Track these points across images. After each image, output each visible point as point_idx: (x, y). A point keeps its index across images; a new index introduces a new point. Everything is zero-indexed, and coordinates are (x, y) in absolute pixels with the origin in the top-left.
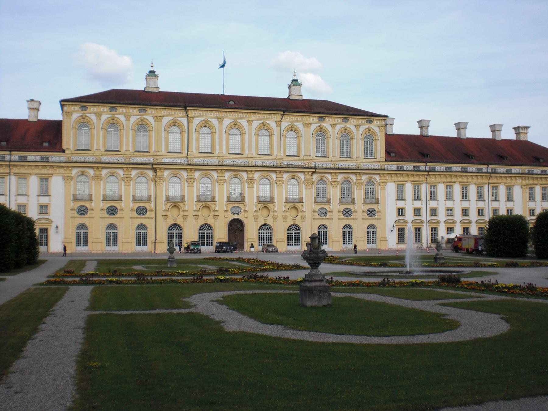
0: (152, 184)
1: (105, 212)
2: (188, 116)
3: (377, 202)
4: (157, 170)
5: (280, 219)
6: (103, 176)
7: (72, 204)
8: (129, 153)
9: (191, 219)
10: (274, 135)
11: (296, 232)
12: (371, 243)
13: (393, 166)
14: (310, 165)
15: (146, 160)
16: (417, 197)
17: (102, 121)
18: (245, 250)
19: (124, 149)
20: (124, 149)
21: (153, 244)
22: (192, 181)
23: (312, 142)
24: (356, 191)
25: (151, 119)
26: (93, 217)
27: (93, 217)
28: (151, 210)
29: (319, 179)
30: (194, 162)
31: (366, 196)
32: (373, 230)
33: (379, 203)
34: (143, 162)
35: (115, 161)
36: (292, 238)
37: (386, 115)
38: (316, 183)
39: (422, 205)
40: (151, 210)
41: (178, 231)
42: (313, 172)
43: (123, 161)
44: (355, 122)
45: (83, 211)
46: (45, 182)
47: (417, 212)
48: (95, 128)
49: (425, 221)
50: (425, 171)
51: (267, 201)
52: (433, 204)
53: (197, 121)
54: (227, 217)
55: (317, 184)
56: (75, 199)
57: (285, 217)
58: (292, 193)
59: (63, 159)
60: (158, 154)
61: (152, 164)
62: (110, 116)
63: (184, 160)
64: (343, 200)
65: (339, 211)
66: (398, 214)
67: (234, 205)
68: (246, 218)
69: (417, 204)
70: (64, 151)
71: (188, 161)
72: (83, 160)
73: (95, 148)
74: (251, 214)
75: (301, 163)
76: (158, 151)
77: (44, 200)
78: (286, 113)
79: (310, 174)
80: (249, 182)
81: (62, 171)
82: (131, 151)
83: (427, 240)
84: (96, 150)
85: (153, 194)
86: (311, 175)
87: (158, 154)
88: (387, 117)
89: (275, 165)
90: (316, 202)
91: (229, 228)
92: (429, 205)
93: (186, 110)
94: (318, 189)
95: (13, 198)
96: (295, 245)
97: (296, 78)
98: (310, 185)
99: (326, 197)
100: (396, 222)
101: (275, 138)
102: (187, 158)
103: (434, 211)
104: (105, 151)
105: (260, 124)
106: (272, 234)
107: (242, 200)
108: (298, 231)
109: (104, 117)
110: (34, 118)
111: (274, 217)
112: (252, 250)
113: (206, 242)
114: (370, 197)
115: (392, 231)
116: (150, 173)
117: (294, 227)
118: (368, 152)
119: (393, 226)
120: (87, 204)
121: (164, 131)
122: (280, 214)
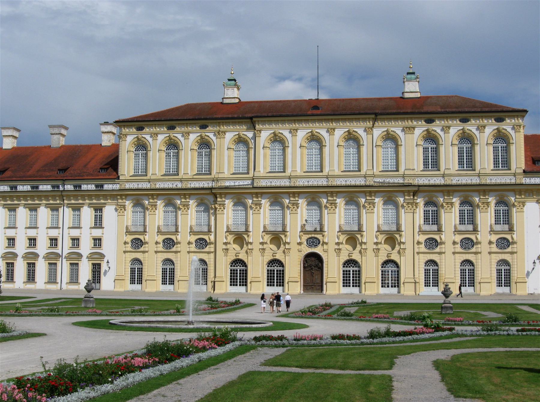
1: (161, 245)
3: (511, 230)
9: (256, 253)
12: (503, 286)
15: (205, 183)
28: (211, 243)
36: (469, 278)
37: (525, 109)
41: (355, 268)
45: (138, 243)
46: (99, 212)
54: (301, 251)
56: (128, 232)
57: (377, 251)
59: (117, 187)
60: (221, 176)
67: (310, 236)
68: (325, 251)
74: (332, 247)
77: (97, 233)
78: (379, 117)
79: (412, 194)
91: (304, 264)
95: (66, 231)
109: (161, 137)
110: (108, 142)
113: (275, 281)
119: (534, 263)
120: (173, 237)
122: (370, 246)
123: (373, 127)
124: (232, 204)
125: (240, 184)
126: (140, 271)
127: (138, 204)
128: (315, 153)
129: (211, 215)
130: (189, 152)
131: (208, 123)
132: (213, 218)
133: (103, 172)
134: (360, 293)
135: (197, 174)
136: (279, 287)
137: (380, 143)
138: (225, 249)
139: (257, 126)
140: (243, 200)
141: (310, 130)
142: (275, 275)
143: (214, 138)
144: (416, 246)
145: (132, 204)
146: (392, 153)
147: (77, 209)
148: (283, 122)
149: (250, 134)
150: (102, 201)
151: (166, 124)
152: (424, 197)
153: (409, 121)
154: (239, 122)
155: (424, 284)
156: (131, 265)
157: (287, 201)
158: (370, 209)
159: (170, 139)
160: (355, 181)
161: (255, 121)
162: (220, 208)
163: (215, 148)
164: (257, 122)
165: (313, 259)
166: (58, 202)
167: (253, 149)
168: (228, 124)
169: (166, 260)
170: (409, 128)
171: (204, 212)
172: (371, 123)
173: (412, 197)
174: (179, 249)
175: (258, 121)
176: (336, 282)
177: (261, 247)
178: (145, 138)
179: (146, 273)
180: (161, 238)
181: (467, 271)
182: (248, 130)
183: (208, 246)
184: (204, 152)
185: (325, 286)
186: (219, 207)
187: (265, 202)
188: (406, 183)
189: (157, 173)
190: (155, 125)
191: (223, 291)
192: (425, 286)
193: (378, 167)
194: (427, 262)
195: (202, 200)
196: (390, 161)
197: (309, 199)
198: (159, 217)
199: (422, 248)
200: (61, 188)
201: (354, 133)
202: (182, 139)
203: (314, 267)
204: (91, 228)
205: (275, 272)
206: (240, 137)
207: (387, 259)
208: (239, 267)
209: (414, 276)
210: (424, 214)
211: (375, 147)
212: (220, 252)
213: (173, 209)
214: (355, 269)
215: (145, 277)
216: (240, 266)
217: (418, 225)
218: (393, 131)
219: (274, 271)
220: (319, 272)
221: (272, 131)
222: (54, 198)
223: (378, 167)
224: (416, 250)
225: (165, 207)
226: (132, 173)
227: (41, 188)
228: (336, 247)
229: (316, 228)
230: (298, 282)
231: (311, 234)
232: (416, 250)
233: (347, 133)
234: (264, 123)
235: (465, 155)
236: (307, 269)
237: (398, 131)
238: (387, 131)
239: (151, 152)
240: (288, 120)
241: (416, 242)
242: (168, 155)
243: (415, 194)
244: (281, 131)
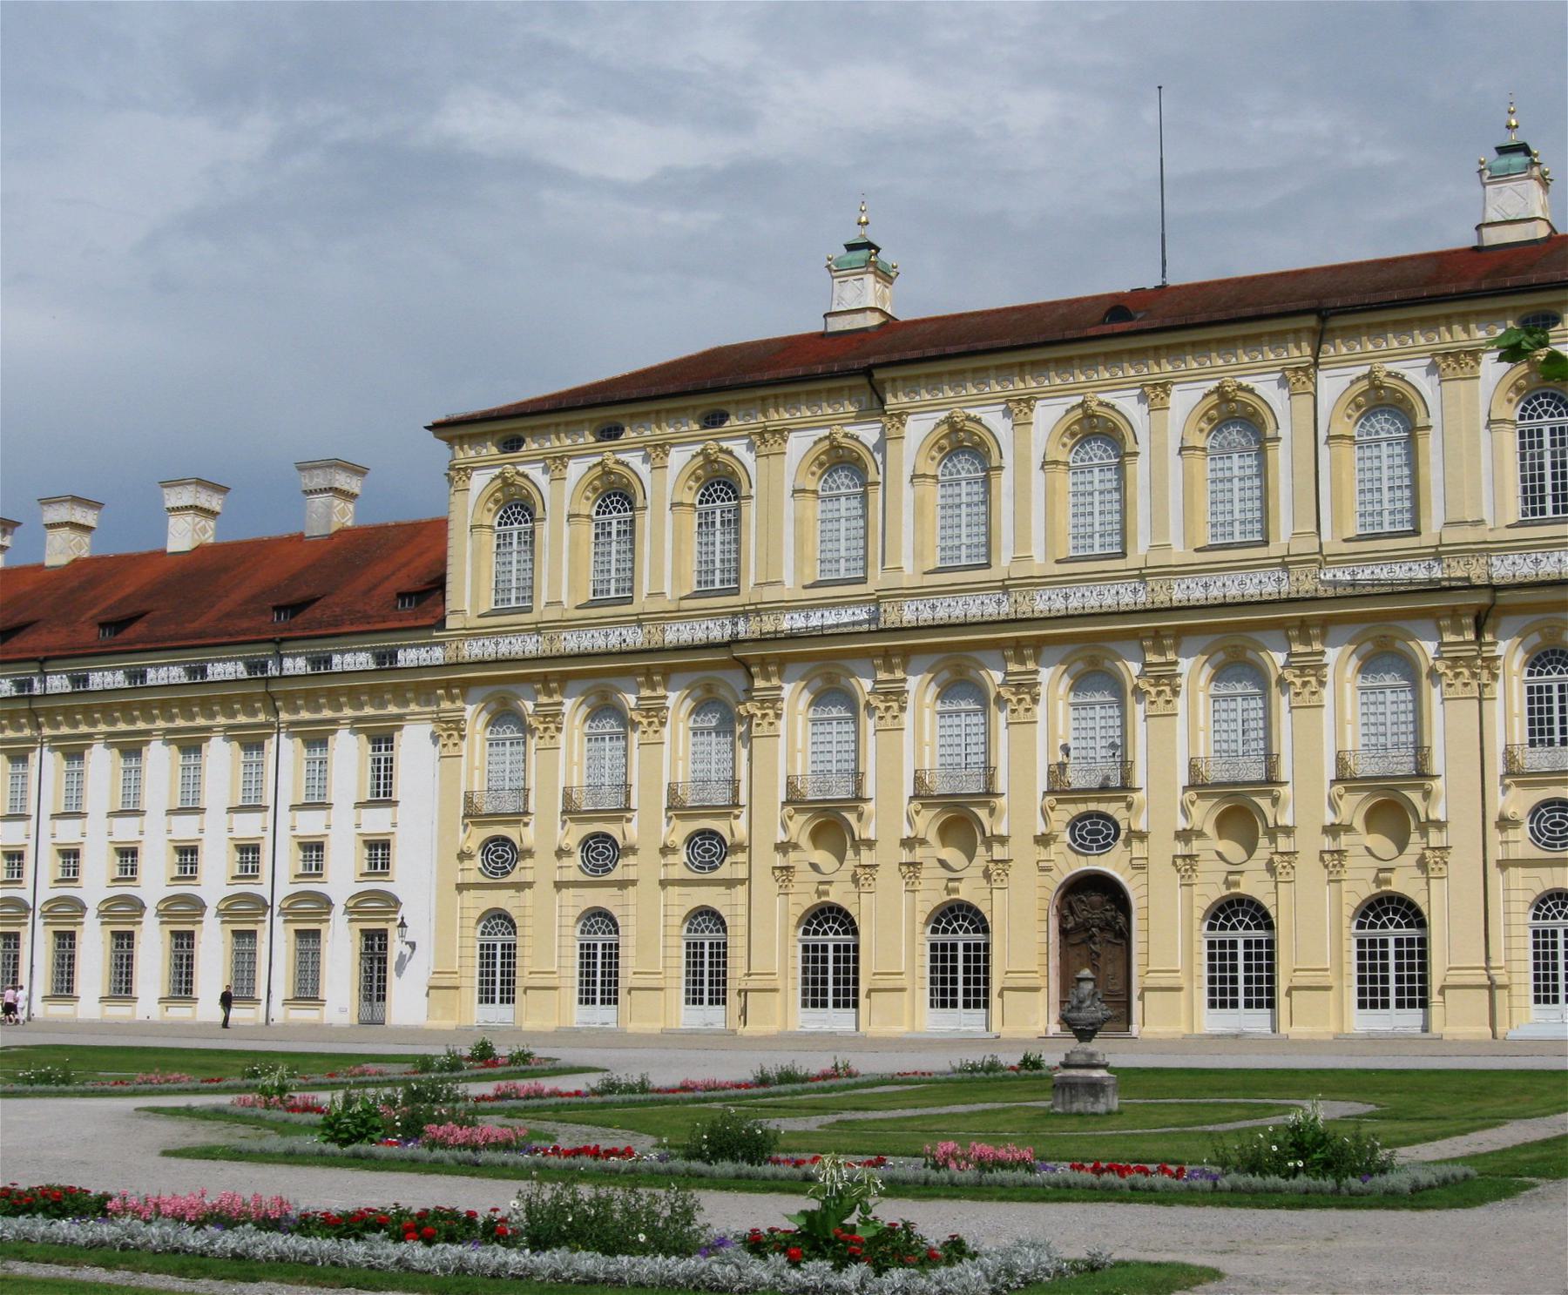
1: (577, 859)
5: (1308, 868)
9: (889, 878)
19: (646, 590)
20: (646, 590)
28: (739, 848)
56: (473, 815)
60: (769, 594)
67: (1082, 808)
68: (1139, 867)
74: (1162, 849)
77: (377, 822)
78: (1335, 322)
79: (1468, 621)
91: (1062, 919)
96: (1400, 1004)
122: (1310, 843)
123: (1316, 364)
124: (806, 697)
125: (856, 618)
126: (720, 952)
127: (504, 715)
128: (1242, 473)
129: (739, 744)
130: (668, 513)
131: (728, 403)
132: (743, 754)
133: (408, 608)
134: (1274, 1031)
135: (696, 595)
136: (972, 1010)
137: (1345, 427)
138: (781, 868)
139: (890, 399)
140: (972, 673)
141: (1079, 399)
142: (960, 964)
143: (748, 458)
144: (1494, 835)
145: (485, 717)
146: (1398, 461)
147: (316, 739)
148: (980, 376)
149: (869, 434)
150: (392, 709)
152: (1523, 634)
153: (1457, 328)
154: (830, 391)
155: (1532, 993)
156: (483, 933)
157: (998, 676)
158: (1306, 691)
159: (607, 473)
160: (1242, 583)
161: (883, 382)
162: (764, 716)
163: (753, 492)
164: (888, 386)
165: (1096, 898)
166: (261, 718)
167: (880, 487)
168: (791, 401)
169: (594, 916)
170: (1456, 355)
171: (718, 734)
172: (1307, 350)
173: (1470, 636)
174: (631, 874)
175: (894, 380)
176: (1179, 989)
177: (905, 856)
178: (526, 477)
179: (527, 961)
180: (573, 835)
182: (861, 417)
183: (728, 860)
184: (718, 512)
185: (1136, 1005)
186: (759, 713)
187: (919, 687)
189: (564, 598)
190: (557, 425)
191: (773, 1028)
192: (1537, 1000)
193: (1337, 522)
194: (1544, 902)
195: (709, 688)
196: (1386, 495)
197: (1079, 666)
198: (674, 750)
199: (1521, 842)
200: (273, 671)
201: (1241, 396)
202: (643, 469)
203: (1102, 930)
204: (360, 805)
205: (961, 953)
206: (835, 447)
207: (1375, 890)
208: (831, 936)
209: (1487, 958)
211: (1326, 443)
212: (764, 882)
213: (618, 726)
214: (1406, 932)
216: (837, 933)
217: (1500, 749)
218: (1396, 376)
219: (954, 947)
220: (1118, 949)
221: (943, 415)
222: (248, 704)
223: (1337, 522)
224: (1496, 853)
225: (593, 721)
226: (488, 604)
227: (153, 677)
228: (1180, 848)
229: (1107, 778)
230: (1036, 989)
231: (1085, 801)
232: (1496, 853)
233: (1214, 399)
234: (911, 384)
236: (1075, 939)
237: (1416, 373)
238: (1370, 376)
239: (546, 524)
240: (998, 368)
241: (1492, 818)
243: (1481, 622)
244: (973, 412)
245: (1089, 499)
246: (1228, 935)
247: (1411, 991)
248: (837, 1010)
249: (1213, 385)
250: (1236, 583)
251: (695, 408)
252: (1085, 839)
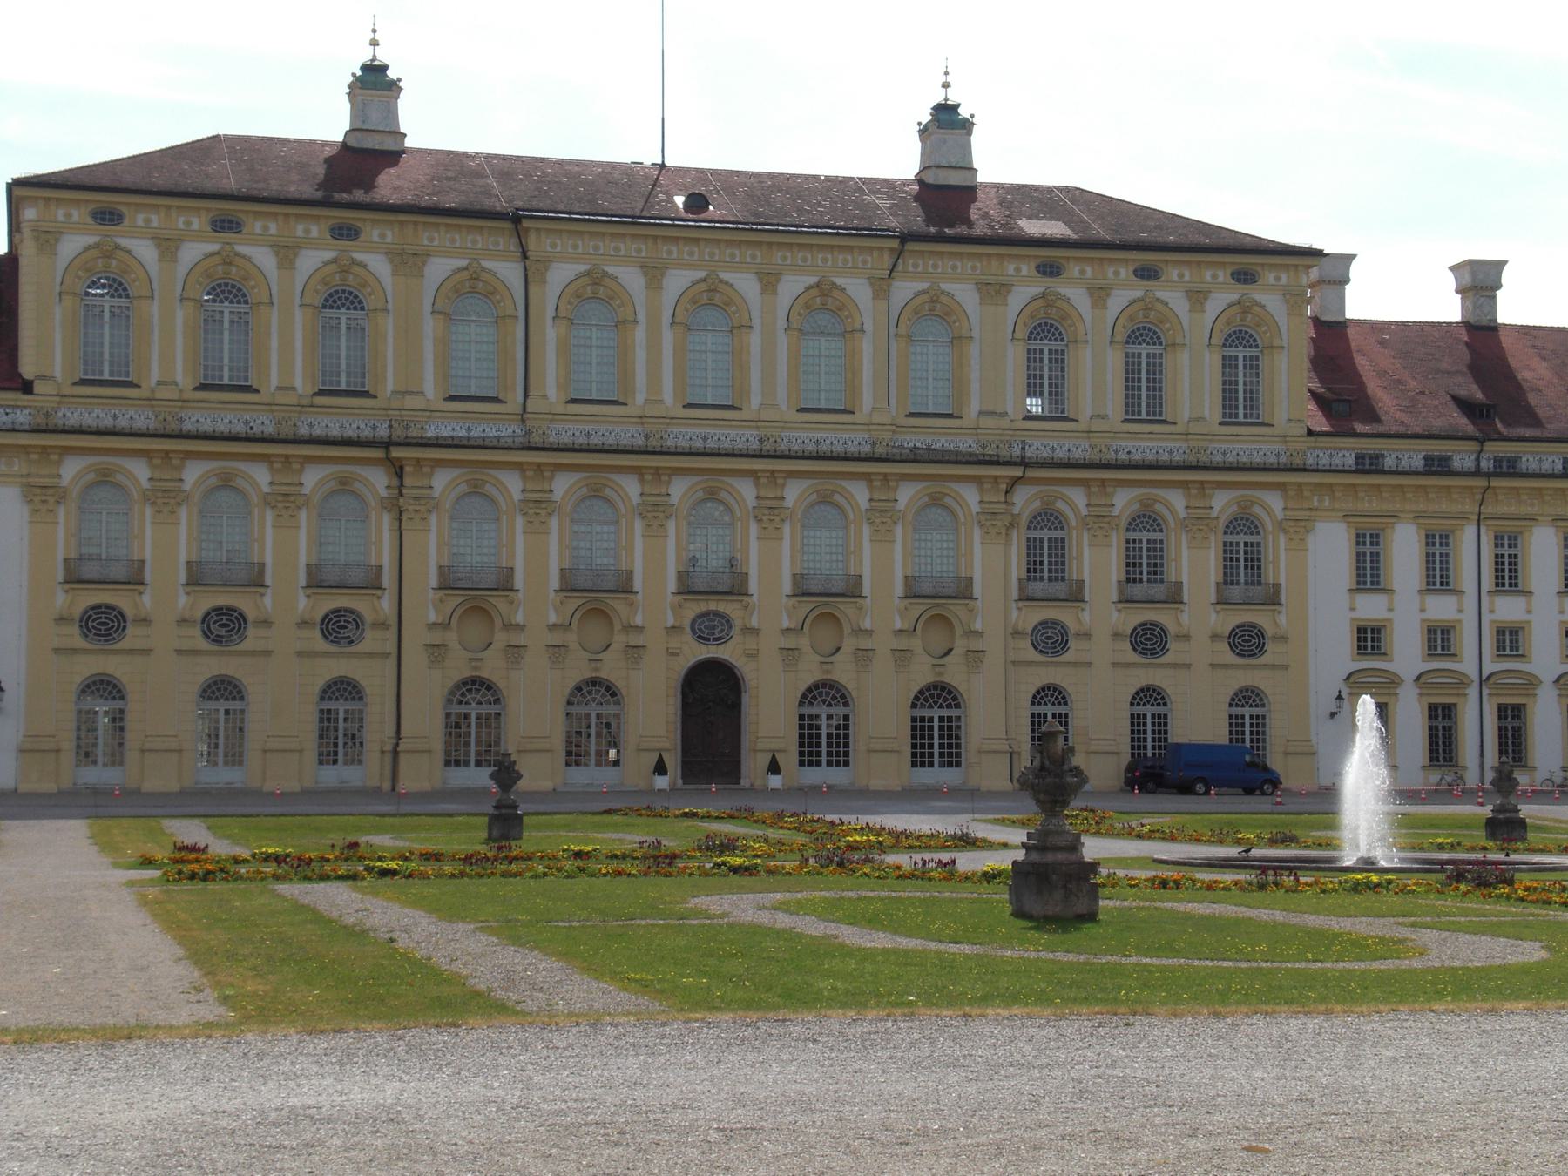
0: (387, 520)
2: (525, 255)
3: (1273, 599)
4: (408, 469)
6: (187, 486)
7: (61, 599)
8: (291, 399)
10: (862, 330)
11: (946, 713)
13: (1344, 453)
14: (1004, 453)
15: (362, 426)
16: (1438, 577)
17: (182, 271)
18: (744, 782)
19: (274, 382)
20: (274, 382)
21: (388, 758)
22: (543, 512)
23: (1014, 359)
24: (1185, 553)
25: (379, 266)
26: (146, 652)
27: (146, 652)
28: (381, 625)
29: (1037, 504)
30: (552, 439)
31: (1225, 574)
32: (1256, 711)
33: (1280, 604)
34: (350, 433)
35: (239, 428)
38: (1024, 521)
39: (1460, 611)
40: (381, 625)
42: (1015, 481)
43: (270, 430)
44: (1187, 278)
47: (1439, 639)
48: (156, 294)
49: (1474, 676)
50: (1477, 473)
51: (834, 590)
52: (1508, 609)
53: (561, 274)
54: (677, 655)
55: (1029, 528)
57: (902, 657)
58: (929, 560)
59: (22, 417)
60: (410, 402)
61: (387, 444)
62: (215, 247)
63: (510, 430)
64: (1137, 590)
65: (1116, 635)
66: (1359, 648)
67: (703, 607)
69: (1441, 608)
70: (27, 387)
71: (528, 433)
72: (107, 422)
73: (155, 375)
75: (966, 444)
76: (411, 393)
78: (910, 246)
79: (1004, 487)
80: (764, 518)
81: (18, 466)
82: (300, 391)
83: (1482, 755)
84: (159, 383)
85: (387, 560)
86: (1007, 492)
87: (410, 402)
88: (1319, 253)
89: (866, 449)
90: (1025, 598)
92: (1492, 611)
93: (520, 235)
94: (1033, 545)
97: (952, 100)
98: (1003, 531)
99: (1063, 579)
100: (1348, 678)
101: (866, 346)
102: (523, 421)
103: (1510, 639)
104: (195, 389)
105: (807, 289)
106: (851, 722)
107: (738, 589)
108: (953, 713)
111: (864, 656)
112: (775, 782)
114: (1242, 579)
115: (1333, 715)
116: (378, 481)
117: (939, 694)
118: (1237, 399)
119: (1339, 697)
120: (121, 600)
121: (433, 312)
131: (365, 220)
139: (532, 243)
151: (208, 210)
161: (527, 230)
181: (1149, 721)
188: (991, 455)
189: (179, 378)
210: (1029, 548)
212: (414, 657)
215: (132, 736)
235: (1144, 376)
242: (213, 321)
245: (704, 356)
246: (926, 713)
247: (838, 754)
248: (830, 768)
249: (813, 280)
250: (1080, 450)
251: (327, 217)
252: (704, 632)
